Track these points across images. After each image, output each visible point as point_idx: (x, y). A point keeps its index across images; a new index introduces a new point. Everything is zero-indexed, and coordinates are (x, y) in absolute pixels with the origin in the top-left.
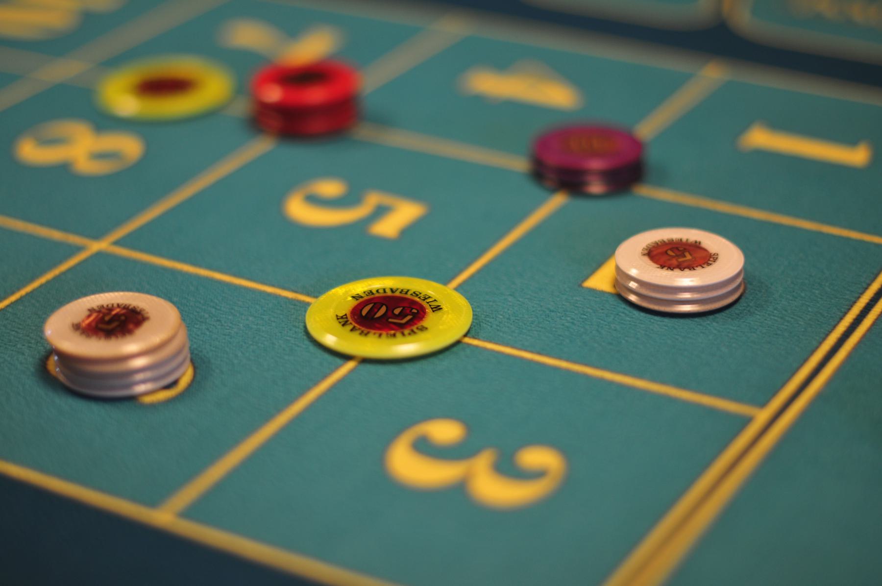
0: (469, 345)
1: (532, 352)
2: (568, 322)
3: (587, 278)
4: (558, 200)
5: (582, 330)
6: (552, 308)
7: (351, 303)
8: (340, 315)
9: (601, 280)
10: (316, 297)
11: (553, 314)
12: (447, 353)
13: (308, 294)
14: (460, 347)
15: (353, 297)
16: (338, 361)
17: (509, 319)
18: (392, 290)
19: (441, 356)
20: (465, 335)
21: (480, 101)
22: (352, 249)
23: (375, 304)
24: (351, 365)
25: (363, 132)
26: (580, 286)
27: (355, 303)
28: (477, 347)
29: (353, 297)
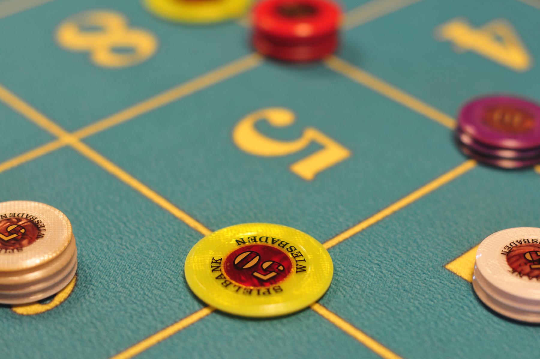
0: (316, 312)
1: (366, 334)
2: (415, 306)
3: (448, 263)
4: (469, 165)
5: (423, 318)
6: (407, 287)
7: (234, 247)
8: (216, 259)
9: (461, 267)
10: (213, 231)
11: (405, 293)
12: (293, 318)
13: (207, 226)
14: (308, 312)
15: (237, 241)
16: (196, 305)
17: (363, 291)
18: (273, 239)
19: (285, 321)
20: (317, 302)
21: (449, 46)
22: (268, 185)
23: (252, 252)
24: (205, 312)
25: (335, 63)
26: (444, 267)
27: (237, 247)
28: (321, 316)
29: (237, 241)
